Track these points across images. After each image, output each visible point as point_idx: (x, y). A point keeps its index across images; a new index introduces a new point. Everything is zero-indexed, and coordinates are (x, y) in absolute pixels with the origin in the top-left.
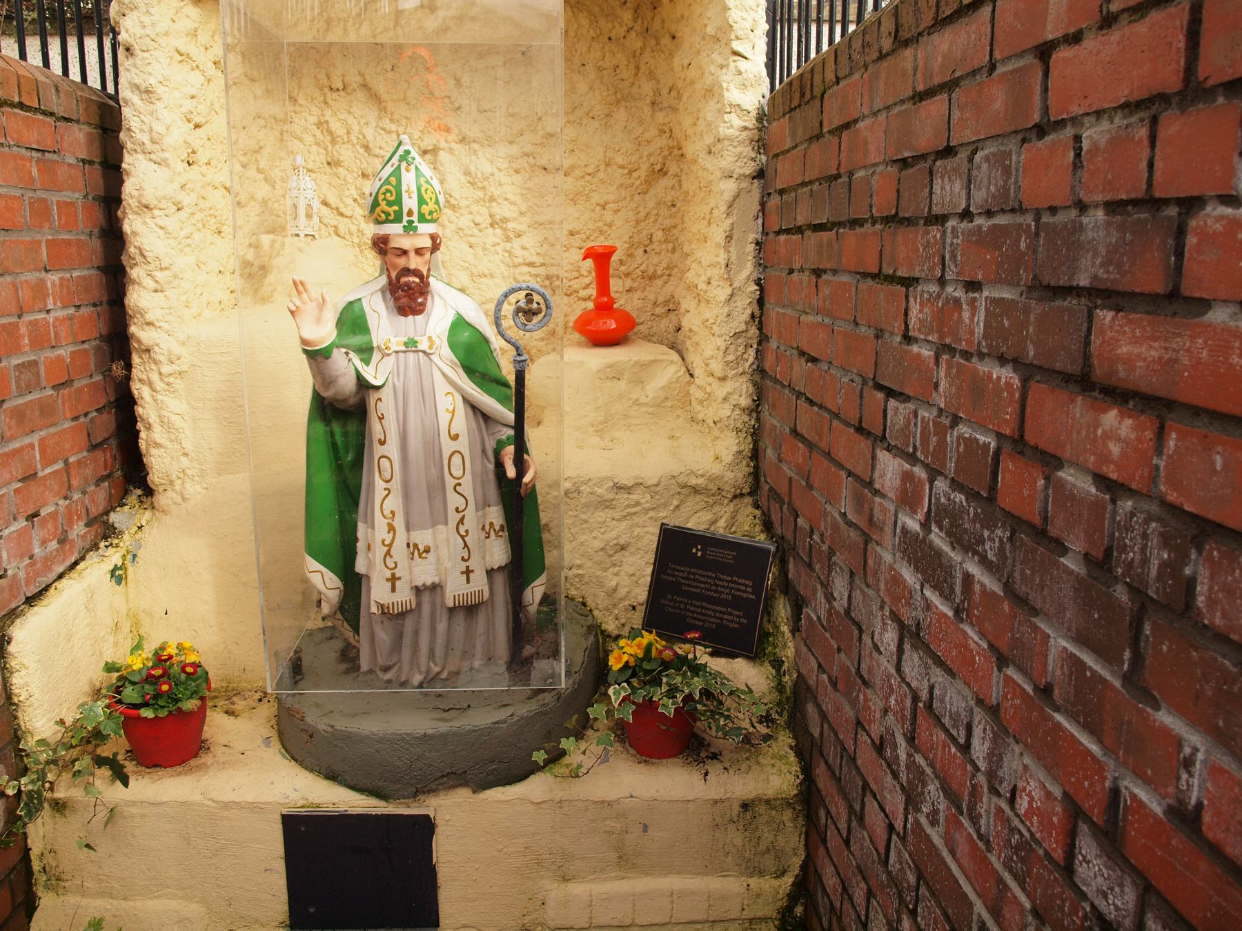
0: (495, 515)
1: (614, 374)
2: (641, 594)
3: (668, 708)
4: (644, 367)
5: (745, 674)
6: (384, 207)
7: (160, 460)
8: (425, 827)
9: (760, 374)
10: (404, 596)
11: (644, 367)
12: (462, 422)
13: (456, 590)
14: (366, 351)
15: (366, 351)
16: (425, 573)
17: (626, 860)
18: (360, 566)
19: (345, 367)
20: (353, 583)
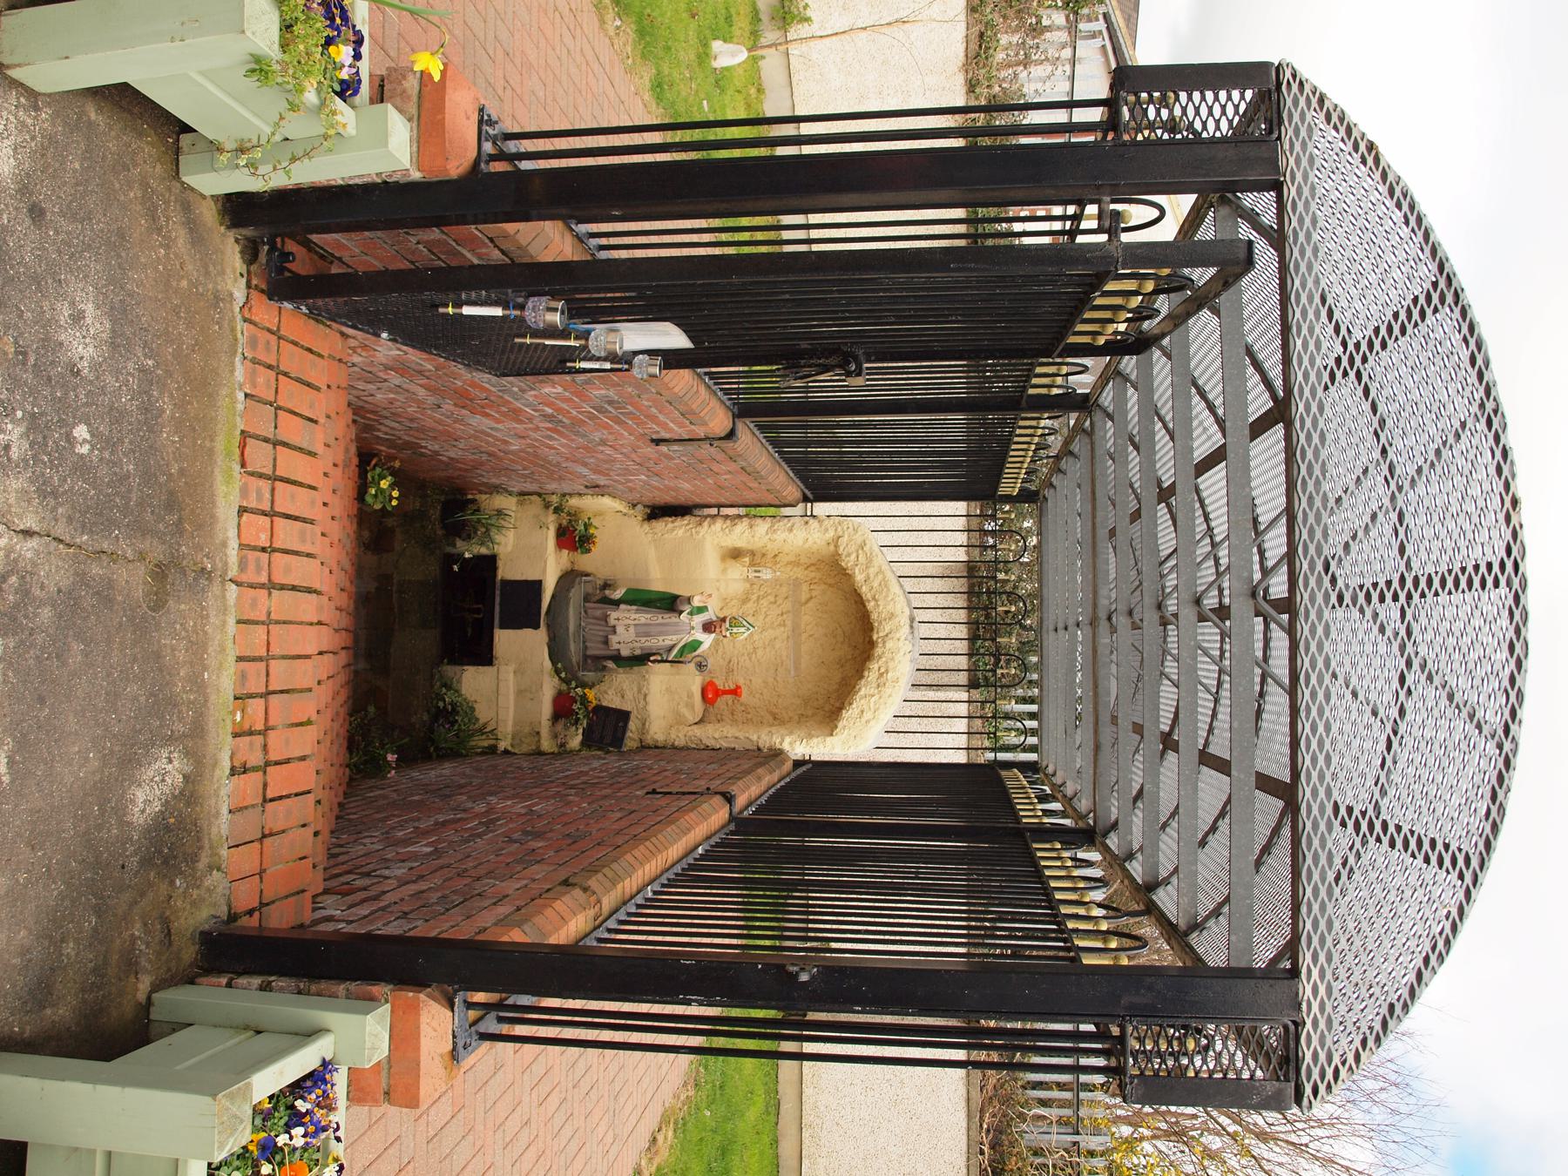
0: (638, 652)
1: (690, 696)
2: (605, 704)
3: (575, 707)
4: (691, 706)
5: (575, 741)
6: (735, 622)
7: (661, 525)
8: (536, 627)
9: (686, 748)
10: (612, 622)
11: (691, 706)
12: (668, 643)
13: (614, 639)
14: (691, 613)
15: (691, 613)
16: (620, 629)
17: (520, 693)
18: (622, 606)
19: (688, 609)
20: (616, 603)
